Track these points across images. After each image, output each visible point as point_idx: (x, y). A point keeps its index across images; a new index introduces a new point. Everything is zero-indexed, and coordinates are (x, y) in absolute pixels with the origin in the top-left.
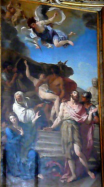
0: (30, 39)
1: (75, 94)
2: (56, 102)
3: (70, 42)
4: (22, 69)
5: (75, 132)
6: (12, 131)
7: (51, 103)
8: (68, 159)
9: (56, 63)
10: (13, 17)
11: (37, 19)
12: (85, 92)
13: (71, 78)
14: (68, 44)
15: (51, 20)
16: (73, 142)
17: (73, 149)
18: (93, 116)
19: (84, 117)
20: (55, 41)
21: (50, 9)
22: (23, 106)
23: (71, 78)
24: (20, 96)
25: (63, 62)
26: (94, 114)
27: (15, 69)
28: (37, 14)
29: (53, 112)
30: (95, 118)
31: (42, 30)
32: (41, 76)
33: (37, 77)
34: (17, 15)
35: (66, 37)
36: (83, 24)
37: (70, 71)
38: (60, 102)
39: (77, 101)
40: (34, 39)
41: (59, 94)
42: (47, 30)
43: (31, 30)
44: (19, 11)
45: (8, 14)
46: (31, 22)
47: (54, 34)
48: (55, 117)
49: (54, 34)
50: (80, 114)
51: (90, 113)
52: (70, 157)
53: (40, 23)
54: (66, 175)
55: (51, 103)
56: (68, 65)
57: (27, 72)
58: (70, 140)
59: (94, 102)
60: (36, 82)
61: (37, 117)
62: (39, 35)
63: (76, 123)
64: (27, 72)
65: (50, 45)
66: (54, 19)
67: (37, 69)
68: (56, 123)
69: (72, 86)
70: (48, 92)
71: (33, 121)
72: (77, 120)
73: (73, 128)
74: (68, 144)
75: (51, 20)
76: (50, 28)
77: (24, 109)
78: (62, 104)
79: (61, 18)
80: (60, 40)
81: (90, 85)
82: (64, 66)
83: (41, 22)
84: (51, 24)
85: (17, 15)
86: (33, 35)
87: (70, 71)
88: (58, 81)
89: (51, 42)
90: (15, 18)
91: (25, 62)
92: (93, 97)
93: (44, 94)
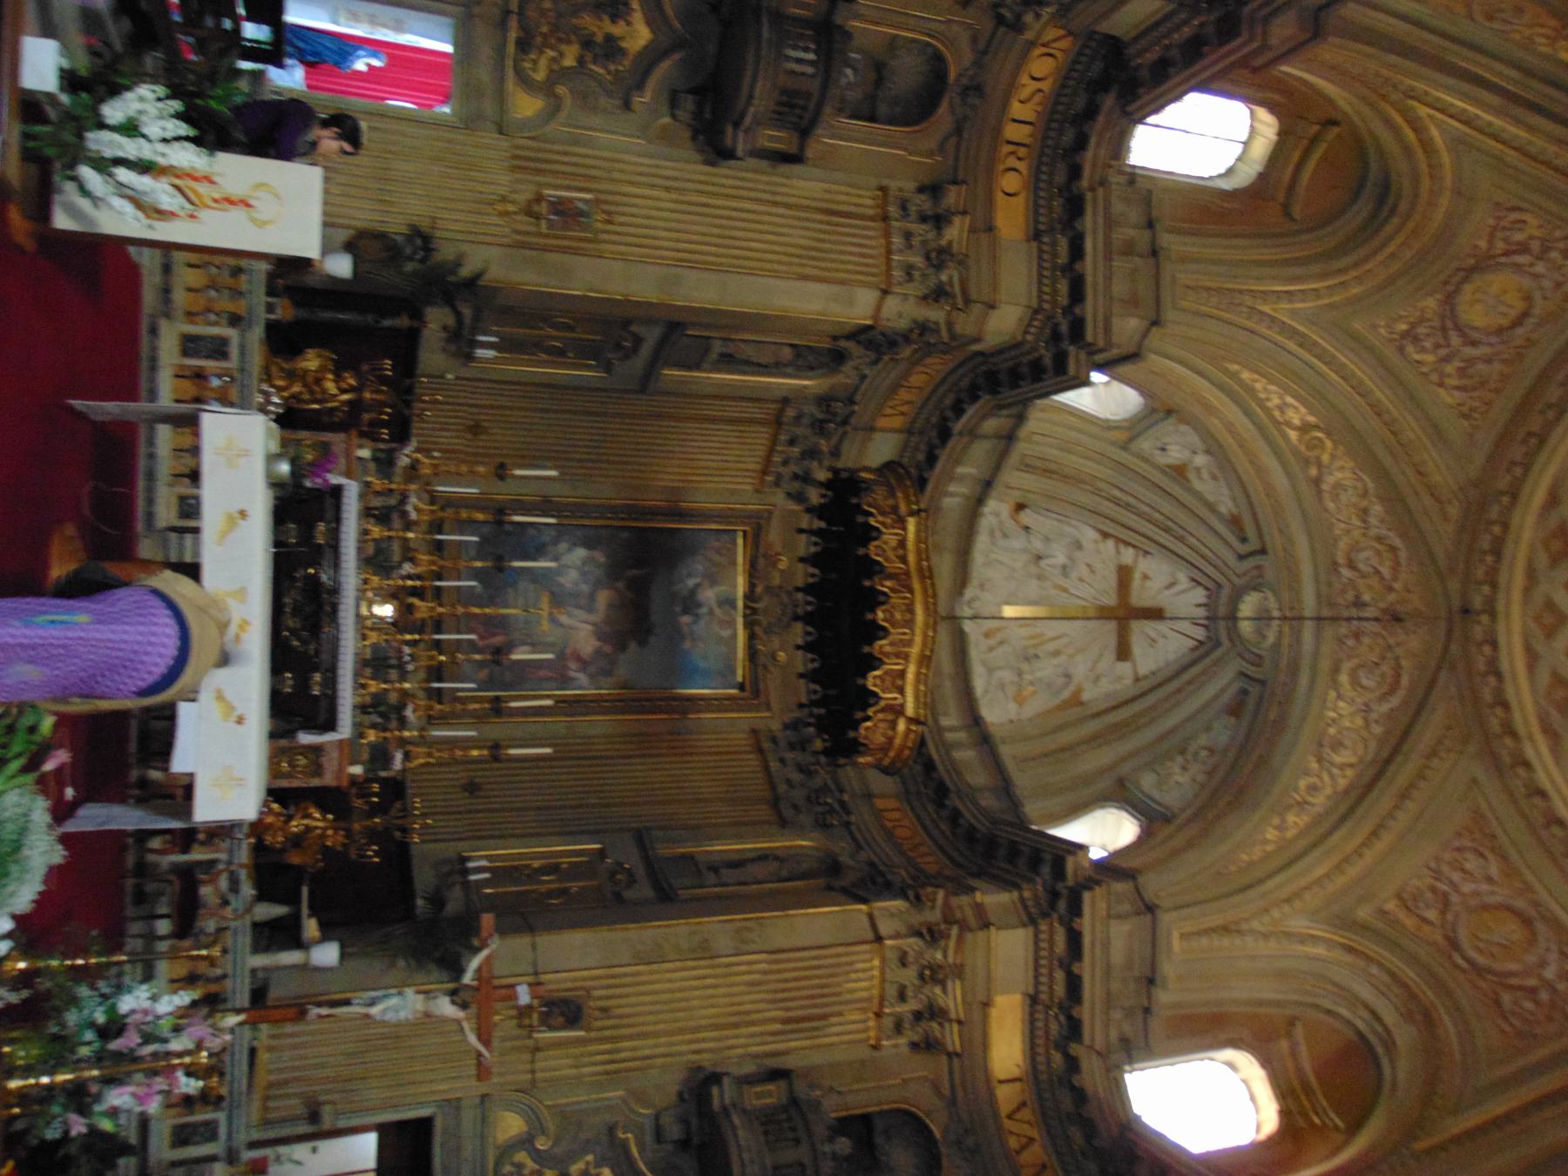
13: (633, 646)
15: (718, 611)
19: (573, 665)
20: (686, 619)
22: (584, 563)
28: (722, 589)
34: (717, 558)
37: (642, 643)
38: (594, 625)
39: (598, 652)
42: (700, 605)
45: (717, 544)
50: (579, 659)
56: (652, 639)
60: (620, 585)
61: (568, 585)
64: (634, 572)
65: (678, 609)
69: (622, 647)
75: (718, 611)
76: (704, 610)
77: (579, 563)
78: (589, 627)
82: (649, 632)
84: (711, 612)
85: (717, 558)
86: (691, 582)
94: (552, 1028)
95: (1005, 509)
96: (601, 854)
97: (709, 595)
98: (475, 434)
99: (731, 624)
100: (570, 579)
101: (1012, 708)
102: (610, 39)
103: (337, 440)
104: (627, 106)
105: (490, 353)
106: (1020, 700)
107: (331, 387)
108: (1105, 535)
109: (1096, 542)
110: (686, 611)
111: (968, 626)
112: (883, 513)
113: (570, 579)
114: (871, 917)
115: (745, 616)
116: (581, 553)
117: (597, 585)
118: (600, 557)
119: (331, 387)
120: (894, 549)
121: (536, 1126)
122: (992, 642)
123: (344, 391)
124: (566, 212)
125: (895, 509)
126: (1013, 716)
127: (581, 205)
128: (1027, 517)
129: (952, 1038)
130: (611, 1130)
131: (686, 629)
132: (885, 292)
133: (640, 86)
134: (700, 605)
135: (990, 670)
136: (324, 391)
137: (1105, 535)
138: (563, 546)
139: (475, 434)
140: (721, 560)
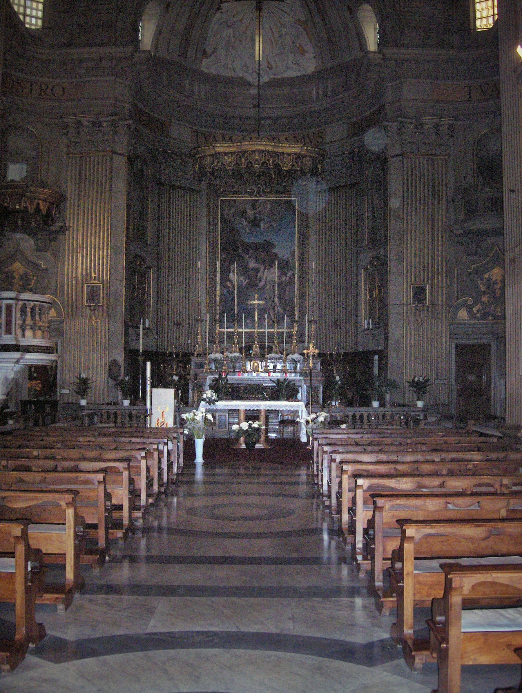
2: (262, 269)
7: (257, 271)
13: (274, 251)
23: (274, 251)
29: (258, 277)
31: (252, 218)
37: (273, 246)
38: (265, 269)
42: (256, 218)
43: (244, 219)
46: (244, 214)
48: (261, 279)
49: (262, 220)
53: (250, 213)
55: (257, 271)
57: (240, 251)
61: (247, 281)
64: (240, 251)
65: (258, 229)
67: (247, 248)
68: (261, 284)
69: (275, 256)
76: (258, 216)
79: (267, 207)
84: (259, 213)
86: (245, 223)
87: (273, 246)
89: (259, 226)
93: (252, 264)
94: (425, 299)
95: (206, 62)
96: (366, 269)
98: (180, 324)
99: (265, 202)
101: (307, 55)
102: (21, 279)
104: (46, 270)
105: (147, 321)
106: (304, 53)
108: (219, 8)
109: (222, 13)
111: (265, 79)
112: (213, 162)
114: (393, 157)
115: (261, 196)
120: (228, 158)
121: (464, 305)
122: (274, 66)
124: (93, 295)
125: (212, 156)
126: (312, 55)
127: (89, 291)
128: (209, 51)
129: (446, 121)
130: (470, 274)
132: (114, 153)
133: (39, 265)
135: (288, 68)
137: (219, 8)
139: (180, 324)
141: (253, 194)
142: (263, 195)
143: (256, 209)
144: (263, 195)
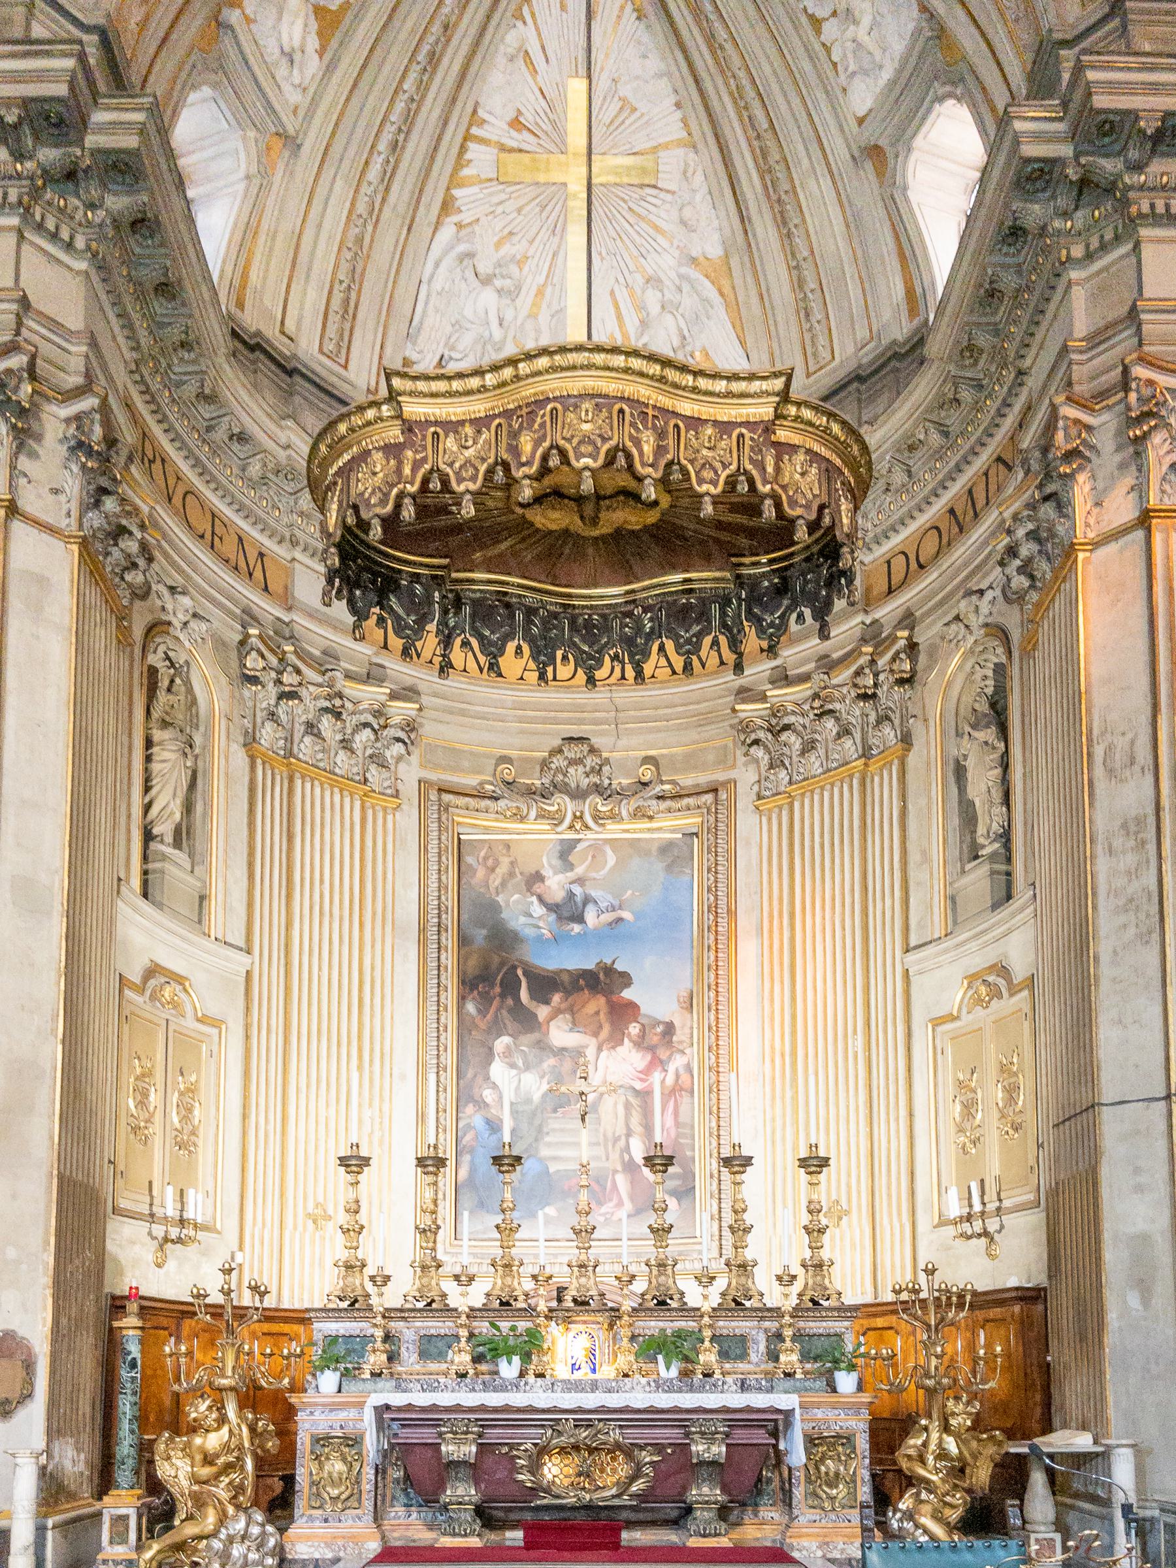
0: (530, 921)
1: (634, 1029)
3: (626, 915)
4: (510, 987)
5: (634, 1113)
6: (488, 1122)
8: (615, 1172)
9: (590, 966)
10: (492, 877)
11: (547, 872)
12: (659, 1023)
13: (627, 994)
14: (620, 920)
15: (579, 870)
16: (629, 1134)
17: (627, 1149)
18: (678, 1076)
20: (590, 916)
21: (580, 847)
22: (513, 1066)
23: (627, 994)
24: (508, 1047)
25: (608, 961)
26: (681, 1071)
27: (498, 990)
30: (685, 1077)
32: (556, 998)
33: (547, 1002)
34: (502, 870)
35: (616, 903)
36: (659, 866)
37: (625, 979)
38: (600, 1049)
39: (640, 1043)
40: (540, 918)
41: (595, 1034)
42: (571, 895)
43: (534, 899)
44: (505, 862)
45: (481, 873)
47: (587, 900)
50: (647, 1071)
51: (672, 1068)
52: (619, 1168)
54: (611, 1204)
56: (619, 967)
58: (621, 1130)
59: (681, 1042)
60: (543, 1012)
61: (545, 1087)
62: (552, 908)
63: (637, 1093)
65: (577, 928)
66: (588, 869)
69: (629, 1010)
70: (571, 1030)
71: (537, 1097)
72: (639, 1086)
73: (628, 1106)
74: (616, 1140)
75: (579, 870)
76: (577, 890)
77: (514, 1072)
78: (604, 1054)
80: (600, 912)
81: (675, 1006)
82: (609, 970)
83: (560, 877)
84: (580, 881)
85: (502, 870)
86: (538, 910)
87: (625, 979)
88: (596, 1004)
90: (495, 881)
91: (520, 972)
92: (678, 1032)
97: (556, 885)
99: (596, 849)
100: (535, 1085)
103: (308, 1425)
107: (213, 1441)
110: (580, 919)
113: (535, 1085)
116: (498, 1069)
117: (543, 1046)
118: (502, 1043)
119: (213, 1441)
123: (222, 1420)
131: (608, 917)
134: (571, 895)
136: (226, 1448)
138: (488, 1095)
140: (505, 862)
141: (561, 822)
142: (591, 823)
143: (570, 867)
144: (591, 823)
